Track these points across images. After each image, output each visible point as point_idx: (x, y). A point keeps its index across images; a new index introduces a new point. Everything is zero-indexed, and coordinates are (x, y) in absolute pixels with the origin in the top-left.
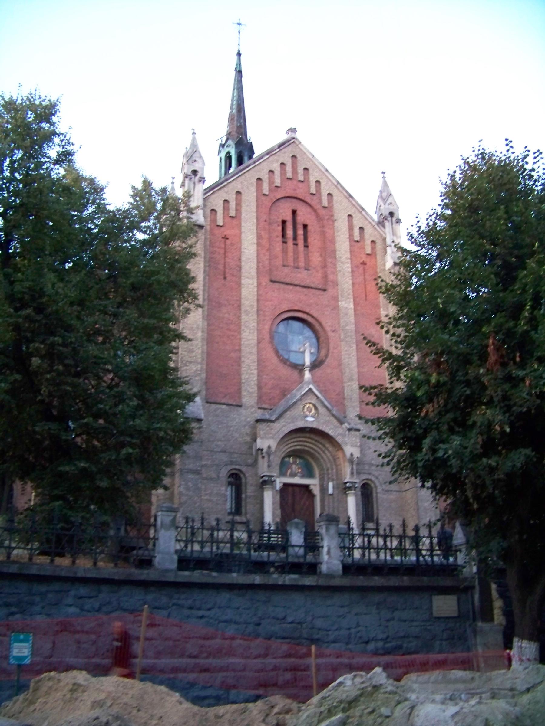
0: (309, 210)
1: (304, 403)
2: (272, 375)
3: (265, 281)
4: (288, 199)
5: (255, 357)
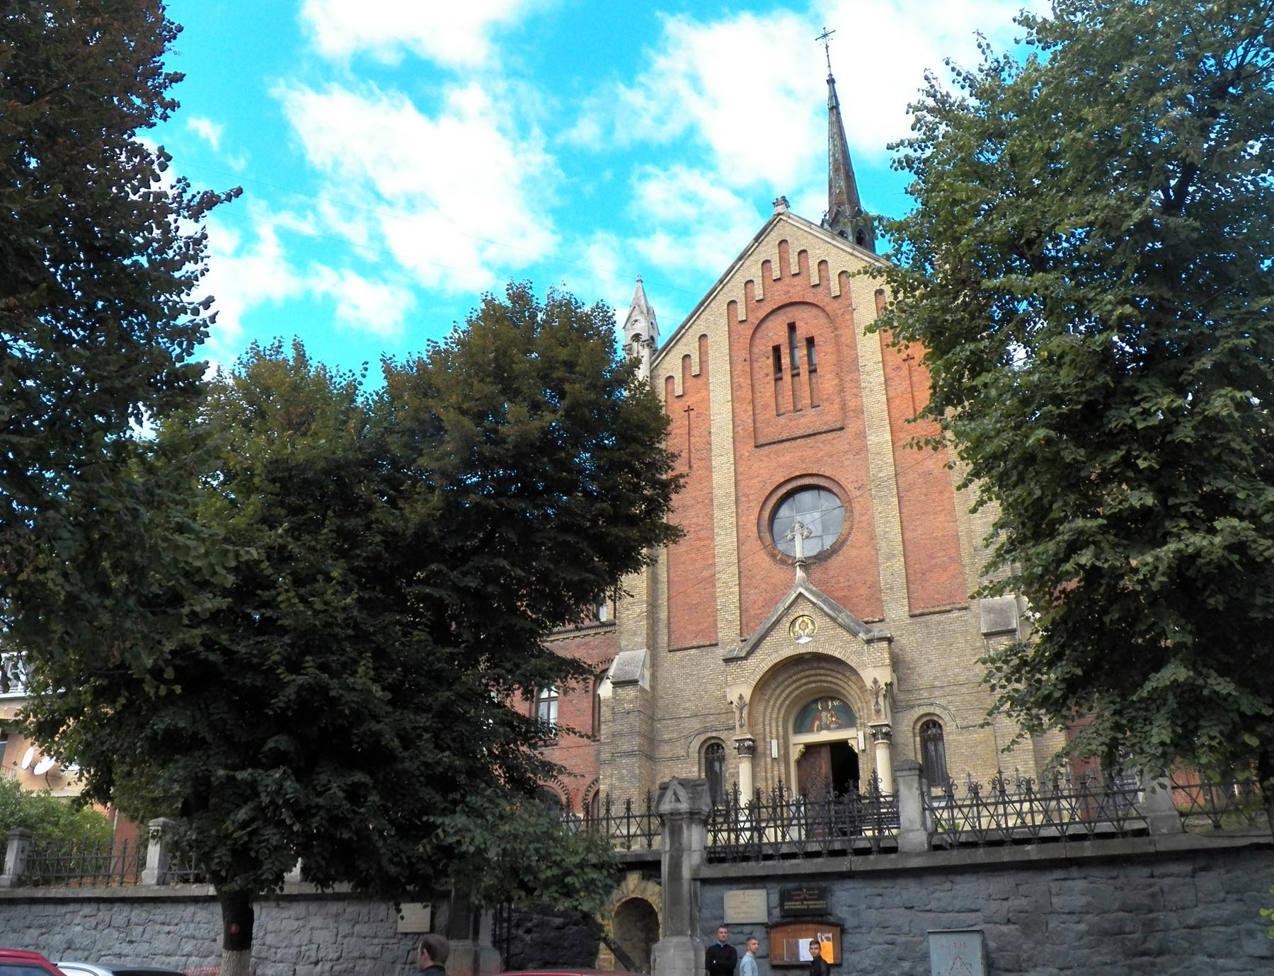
0: (814, 311)
1: (792, 618)
2: (764, 586)
3: (747, 449)
4: (781, 312)
5: (735, 569)
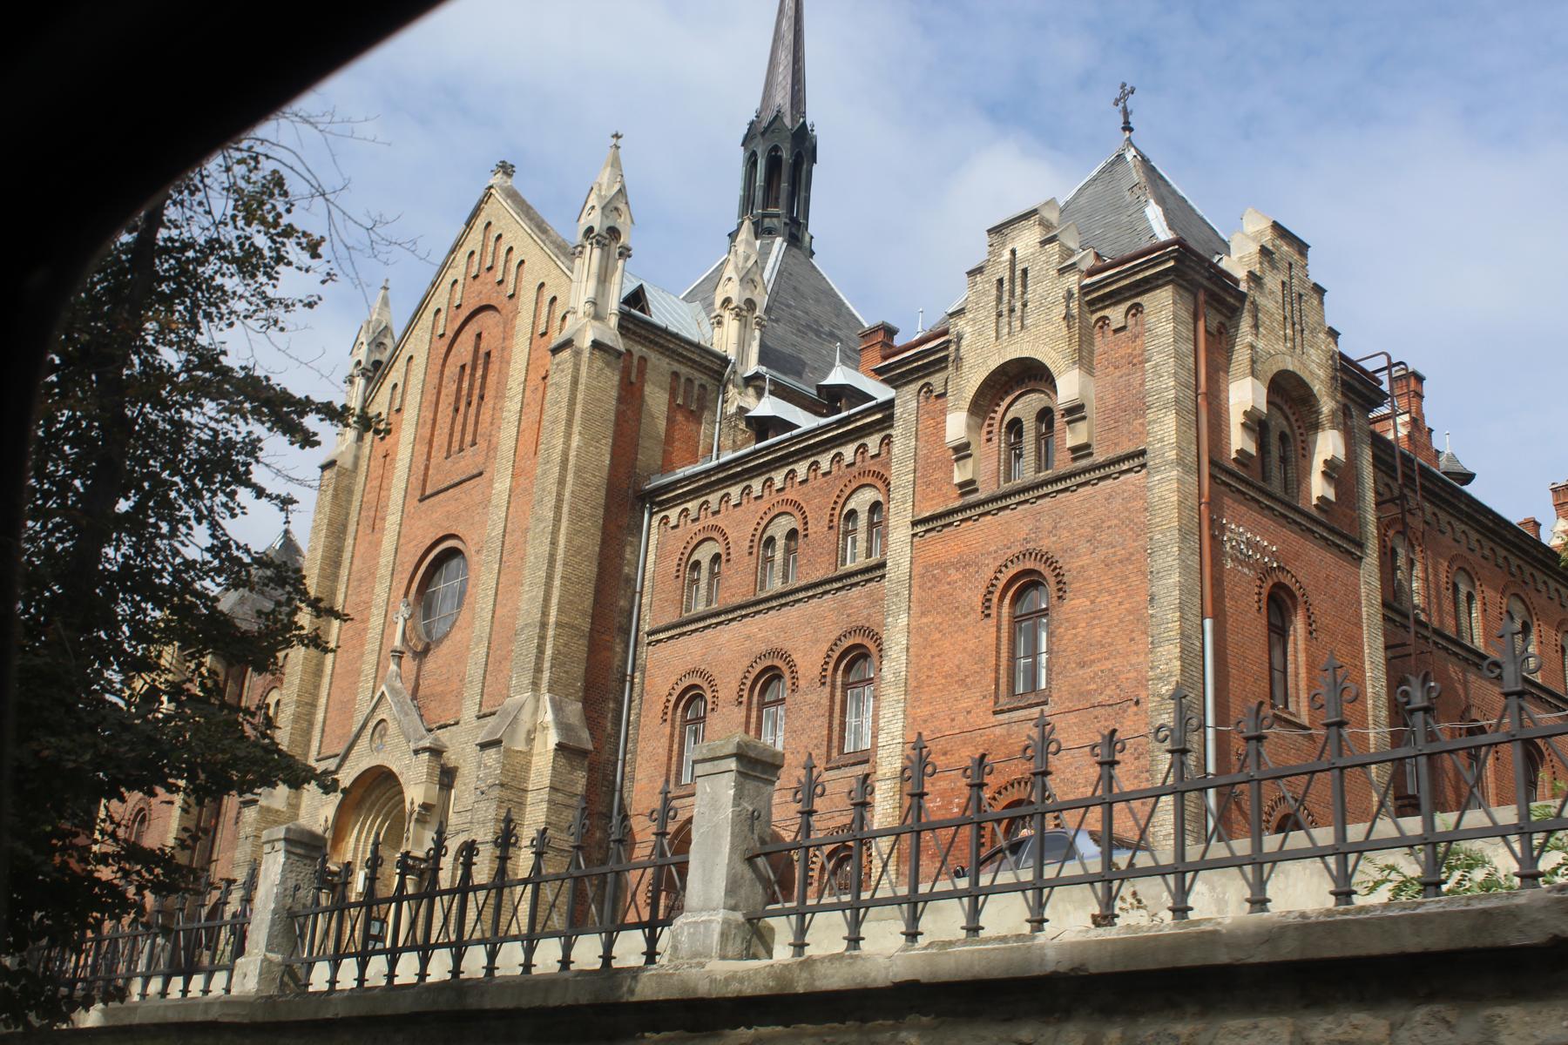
3: (413, 501)
